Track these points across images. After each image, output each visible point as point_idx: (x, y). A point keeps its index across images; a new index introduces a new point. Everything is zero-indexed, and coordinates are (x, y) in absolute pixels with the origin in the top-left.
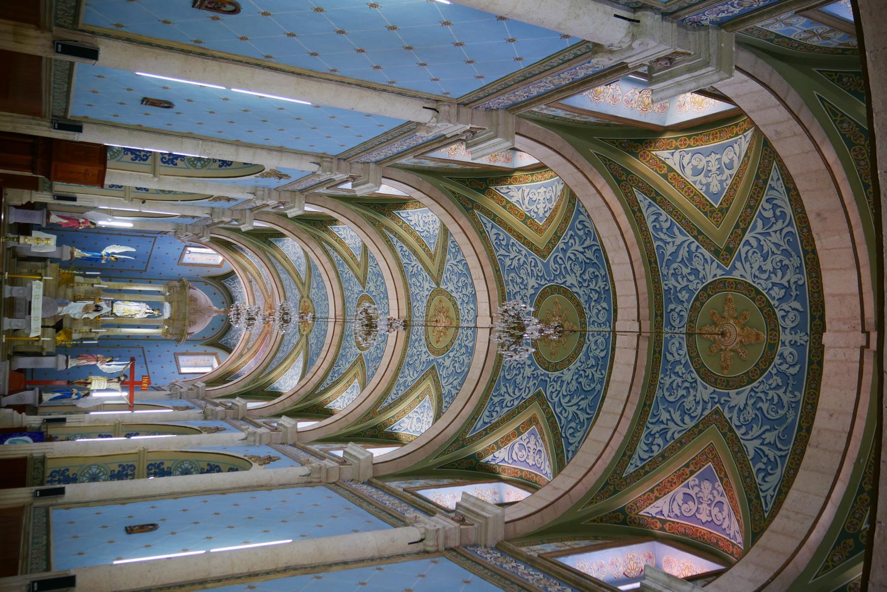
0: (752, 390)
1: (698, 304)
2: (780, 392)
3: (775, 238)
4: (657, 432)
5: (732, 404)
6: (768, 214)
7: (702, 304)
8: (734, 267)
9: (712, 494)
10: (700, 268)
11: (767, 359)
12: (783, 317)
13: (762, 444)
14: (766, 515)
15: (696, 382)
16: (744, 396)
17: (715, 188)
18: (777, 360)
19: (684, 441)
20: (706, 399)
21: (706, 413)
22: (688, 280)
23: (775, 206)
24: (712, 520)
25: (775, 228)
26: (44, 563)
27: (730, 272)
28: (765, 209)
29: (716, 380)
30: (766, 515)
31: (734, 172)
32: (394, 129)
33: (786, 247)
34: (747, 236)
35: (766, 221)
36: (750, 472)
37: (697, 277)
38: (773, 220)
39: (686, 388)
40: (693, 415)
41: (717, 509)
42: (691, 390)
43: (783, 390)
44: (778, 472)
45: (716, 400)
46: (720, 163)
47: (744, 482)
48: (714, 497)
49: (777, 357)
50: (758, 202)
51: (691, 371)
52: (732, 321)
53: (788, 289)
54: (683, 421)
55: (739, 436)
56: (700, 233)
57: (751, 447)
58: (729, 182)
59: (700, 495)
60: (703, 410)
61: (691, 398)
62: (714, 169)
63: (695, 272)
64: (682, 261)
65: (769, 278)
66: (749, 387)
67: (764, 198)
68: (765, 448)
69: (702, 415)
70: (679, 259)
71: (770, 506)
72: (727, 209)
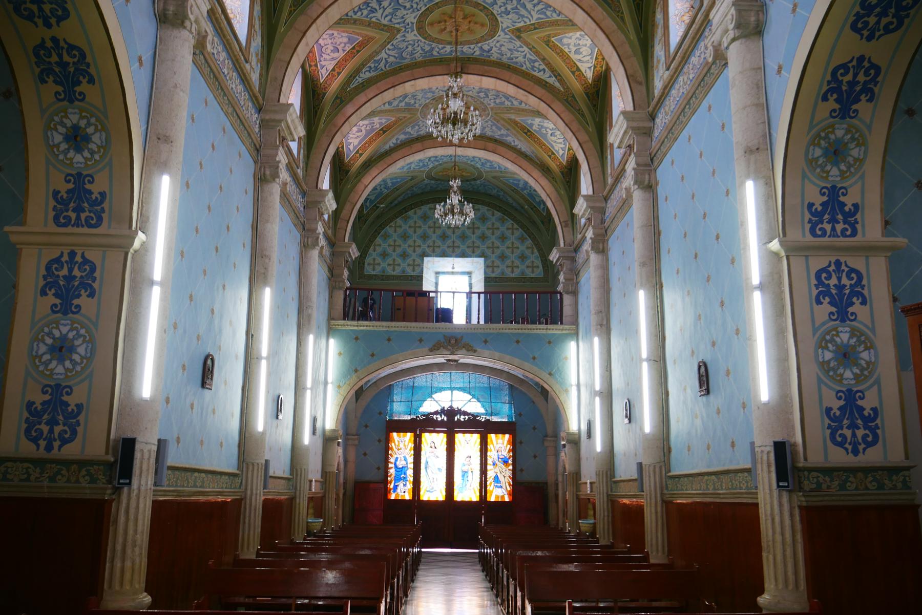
0: (419, 40)
1: (481, 8)
2: (421, 52)
3: (521, 59)
4: (372, 7)
5: (407, 35)
6: (536, 64)
7: (481, 10)
8: (506, 34)
9: (341, 43)
10: (510, 16)
11: (440, 41)
12: (470, 48)
13: (385, 59)
14: (349, 89)
15: (418, 10)
16: (415, 38)
17: (565, 41)
18: (440, 46)
19: (372, 25)
20: (406, 21)
21: (397, 26)
22: (500, 7)
23: (540, 71)
24: (323, 47)
25: (527, 63)
26: (223, 477)
27: (503, 30)
28: (540, 65)
29: (423, 21)
30: (349, 89)
31: (572, 56)
32: (670, 148)
33: (514, 60)
34: (525, 48)
35: (535, 61)
36: (366, 64)
37: (502, 12)
38: (532, 64)
39: (412, 7)
40: (393, 20)
41: (332, 48)
42: (411, 10)
43: (422, 52)
44: (373, 74)
45: (407, 27)
46: (583, 45)
47: (359, 66)
48: (339, 45)
49: (443, 46)
50: (546, 65)
51: (426, 5)
52: (467, 27)
53: (489, 51)
54: (386, 16)
55: (387, 48)
56: (535, 29)
57: (383, 55)
58: (567, 50)
59: (336, 38)
60: (399, 23)
61: (405, 12)
62: (581, 42)
63: (508, 13)
64: (516, 8)
65: (496, 47)
66: (421, 38)
67: (547, 69)
68: (384, 61)
69: (394, 24)
70: (519, 6)
71: (353, 86)
72: (548, 45)
